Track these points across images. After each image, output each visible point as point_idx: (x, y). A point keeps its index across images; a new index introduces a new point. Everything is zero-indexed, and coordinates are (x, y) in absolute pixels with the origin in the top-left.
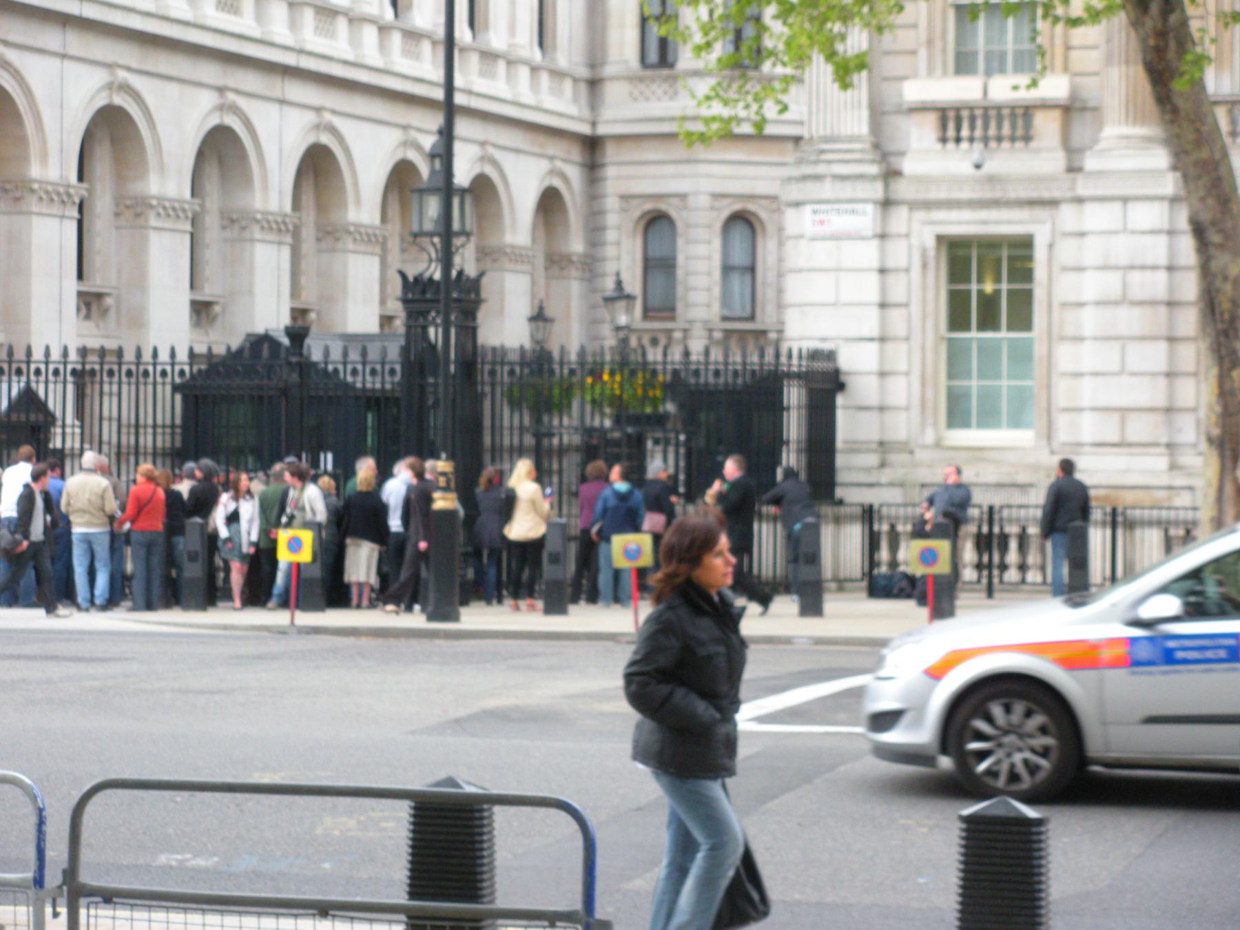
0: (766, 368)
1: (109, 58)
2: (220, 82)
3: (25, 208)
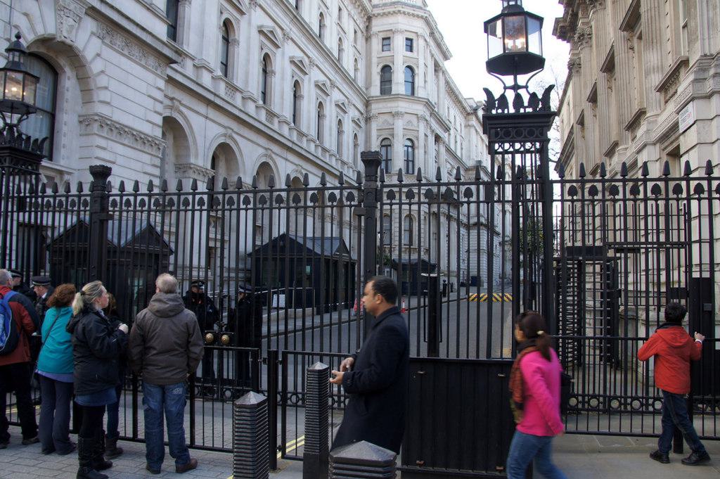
0: (403, 261)
1: (226, 125)
2: (267, 146)
3: (187, 175)
